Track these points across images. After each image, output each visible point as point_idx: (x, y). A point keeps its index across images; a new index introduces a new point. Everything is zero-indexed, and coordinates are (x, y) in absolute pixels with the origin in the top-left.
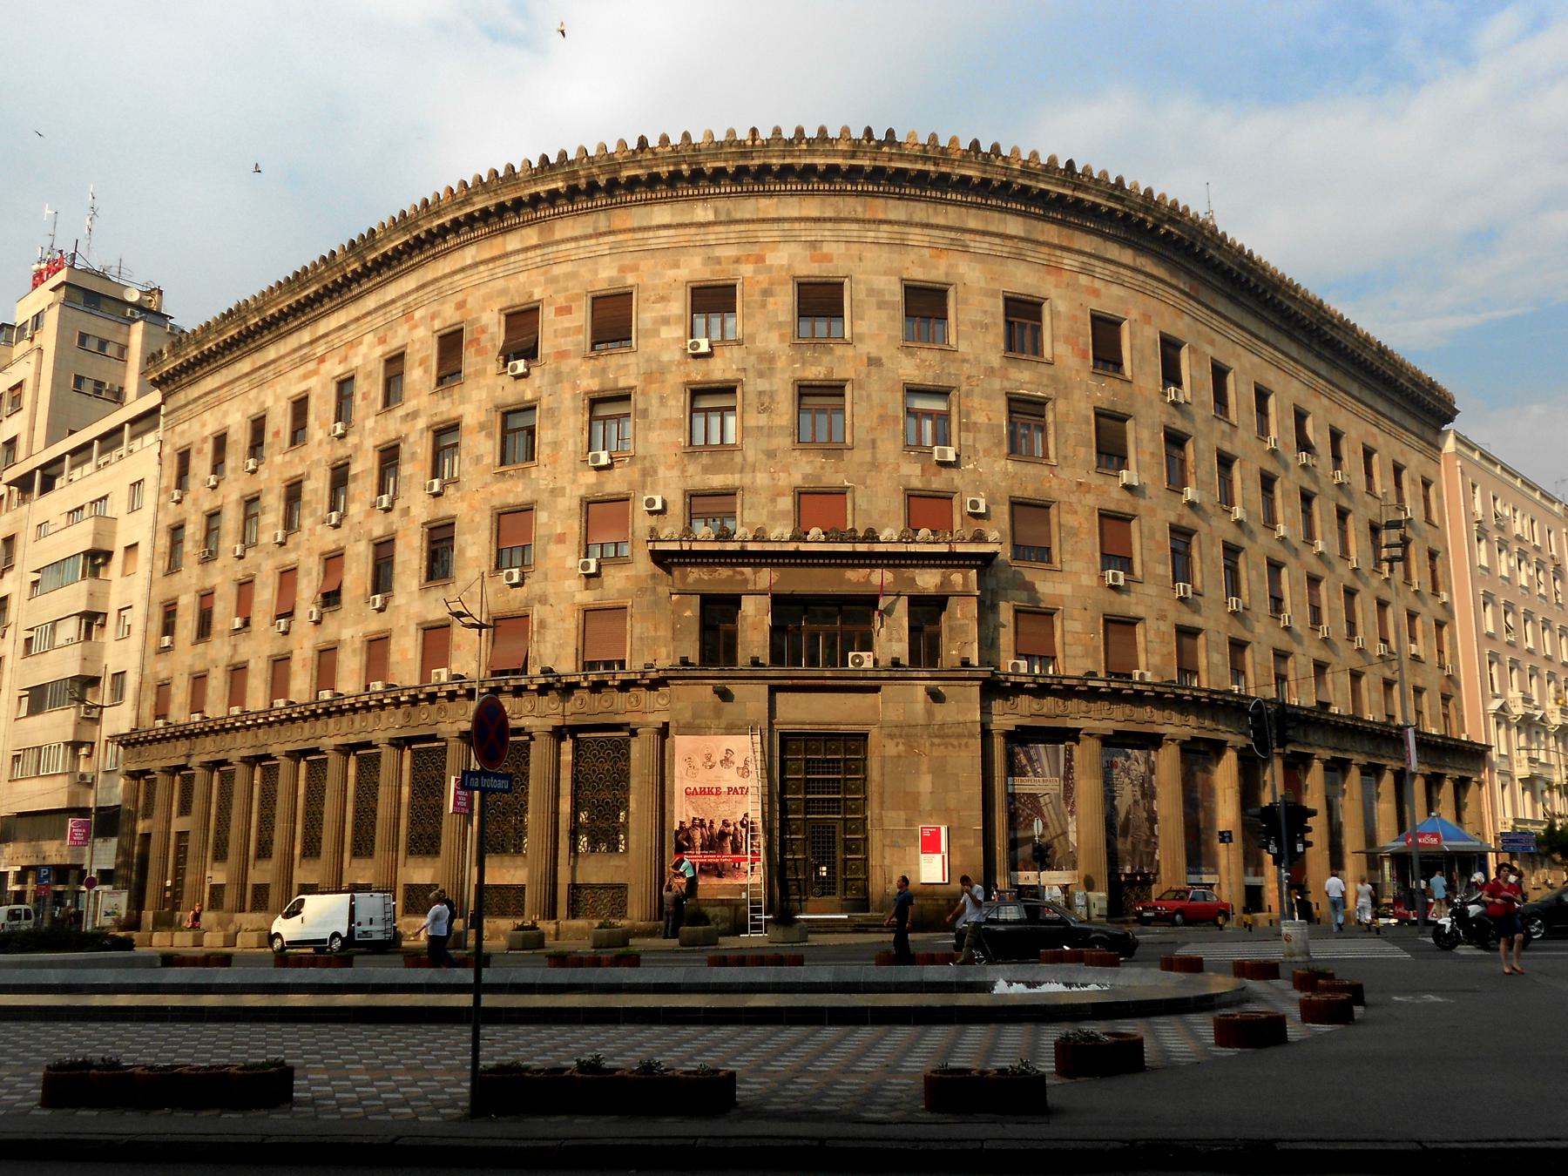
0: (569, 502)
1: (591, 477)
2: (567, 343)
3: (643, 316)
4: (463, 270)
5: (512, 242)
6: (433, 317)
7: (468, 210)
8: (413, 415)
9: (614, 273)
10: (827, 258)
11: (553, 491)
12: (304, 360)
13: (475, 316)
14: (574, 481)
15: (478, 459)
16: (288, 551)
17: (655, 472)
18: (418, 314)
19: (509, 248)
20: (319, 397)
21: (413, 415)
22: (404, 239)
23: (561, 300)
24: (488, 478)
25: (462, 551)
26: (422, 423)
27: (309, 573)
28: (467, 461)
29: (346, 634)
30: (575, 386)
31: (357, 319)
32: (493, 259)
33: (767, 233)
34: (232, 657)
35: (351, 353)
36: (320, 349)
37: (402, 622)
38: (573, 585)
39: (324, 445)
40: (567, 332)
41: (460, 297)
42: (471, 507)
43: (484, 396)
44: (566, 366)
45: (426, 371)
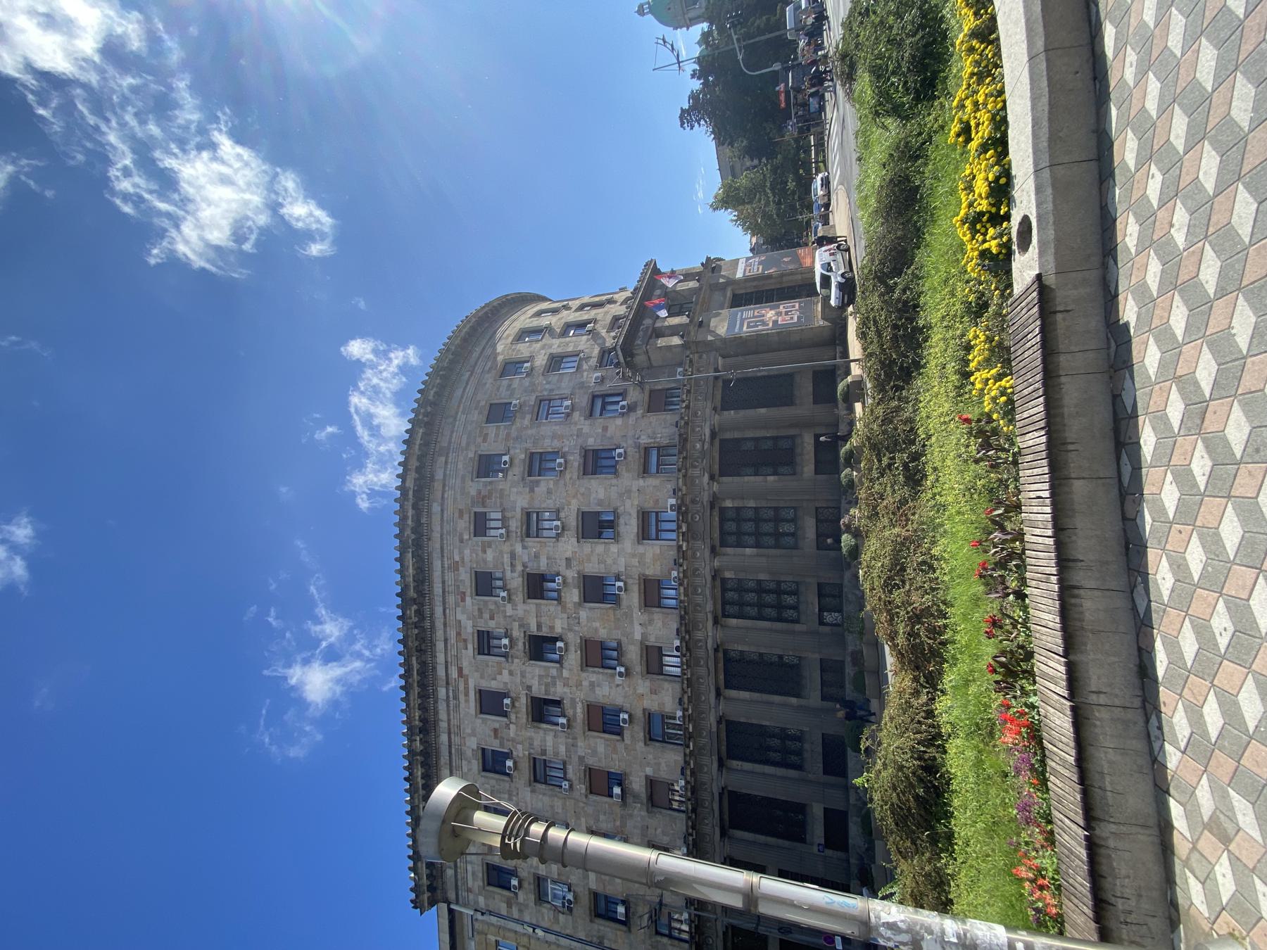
0: (586, 426)
1: (576, 415)
2: (503, 434)
3: (503, 396)
4: (442, 511)
5: (439, 475)
6: (461, 541)
7: (411, 493)
8: (513, 555)
9: (477, 412)
10: (508, 336)
11: (577, 436)
12: (456, 698)
13: (469, 502)
14: (576, 424)
15: (549, 492)
16: (575, 715)
17: (583, 383)
18: (457, 558)
19: (442, 477)
20: (482, 677)
21: (513, 555)
22: (410, 555)
23: (479, 440)
24: (562, 482)
25: (600, 503)
26: (518, 548)
27: (592, 685)
28: (549, 501)
29: (638, 636)
30: (527, 428)
31: (445, 625)
32: (444, 486)
33: (488, 351)
34: (642, 804)
35: (463, 636)
36: (454, 673)
37: (635, 562)
38: (632, 419)
39: (512, 668)
40: (497, 435)
41: (456, 515)
42: (574, 497)
43: (515, 490)
44: (514, 433)
45: (490, 546)
